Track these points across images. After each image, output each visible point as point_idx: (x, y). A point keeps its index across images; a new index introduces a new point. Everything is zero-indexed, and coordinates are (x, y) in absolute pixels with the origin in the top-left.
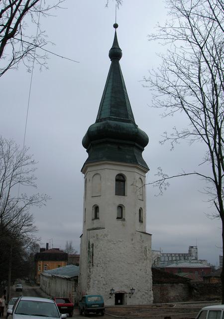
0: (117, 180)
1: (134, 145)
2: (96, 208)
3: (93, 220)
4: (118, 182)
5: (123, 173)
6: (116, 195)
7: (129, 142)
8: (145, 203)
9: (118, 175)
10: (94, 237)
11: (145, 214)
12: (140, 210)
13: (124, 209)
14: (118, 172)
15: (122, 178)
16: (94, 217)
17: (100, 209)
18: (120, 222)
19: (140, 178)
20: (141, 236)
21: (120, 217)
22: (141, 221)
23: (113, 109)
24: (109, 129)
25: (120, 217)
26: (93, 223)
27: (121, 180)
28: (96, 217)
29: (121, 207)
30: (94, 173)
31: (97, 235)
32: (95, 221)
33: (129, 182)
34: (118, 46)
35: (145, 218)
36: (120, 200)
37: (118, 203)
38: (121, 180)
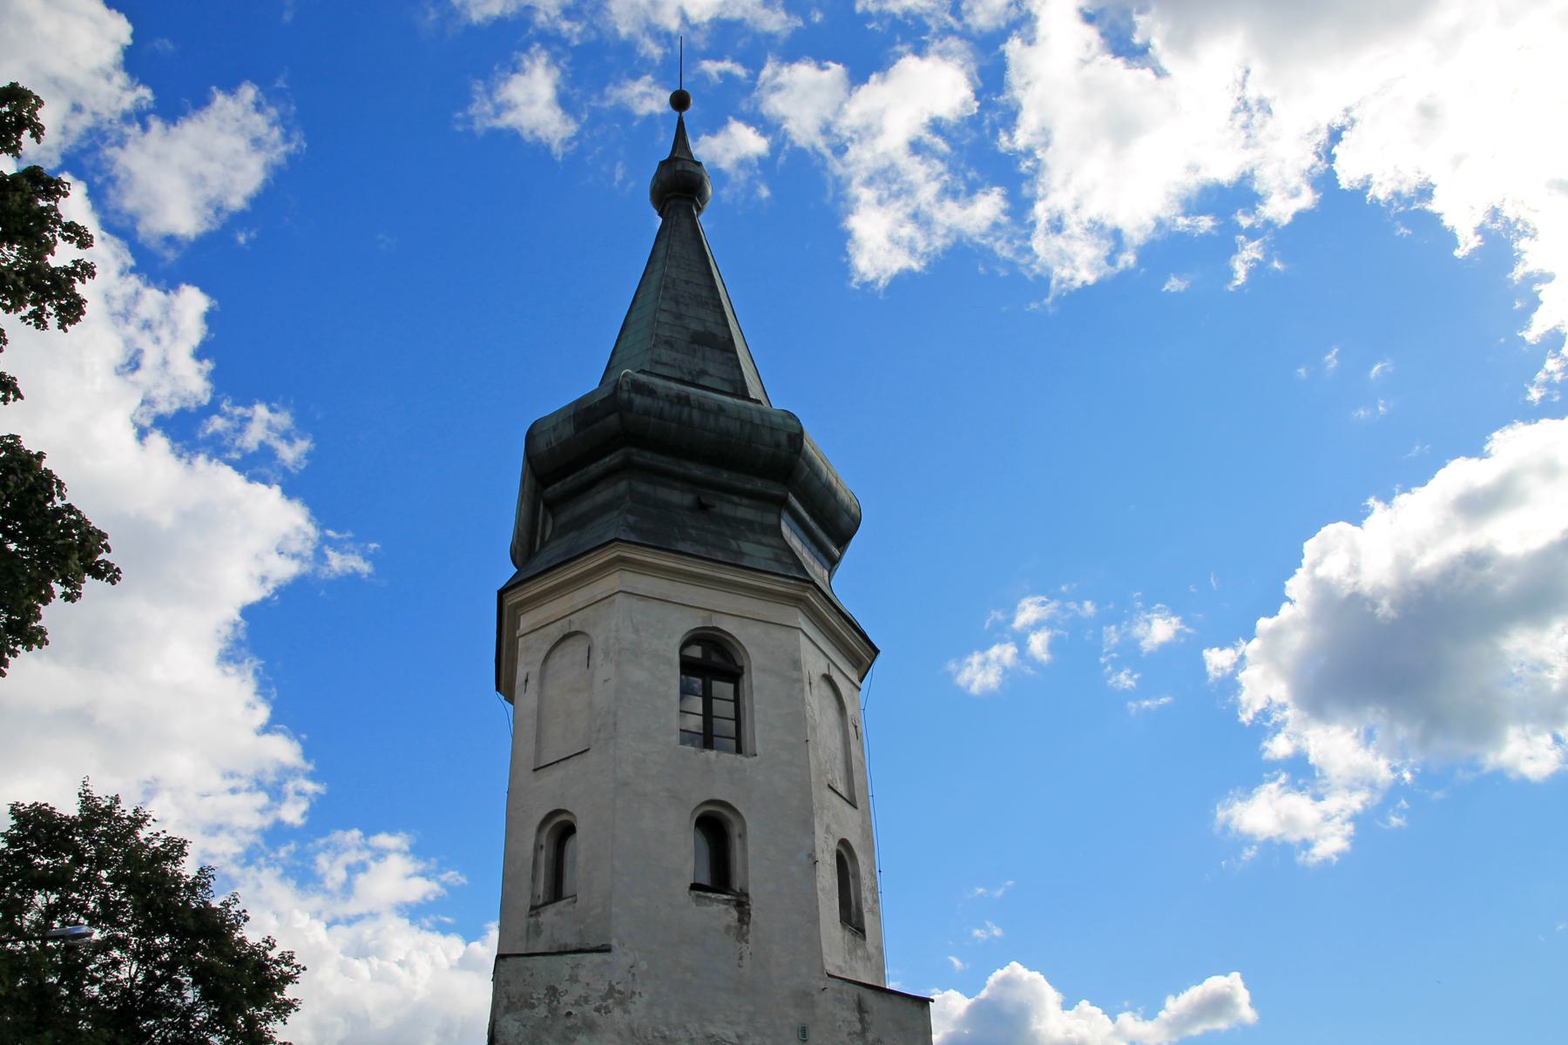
0: (688, 667)
1: (783, 503)
2: (561, 830)
3: (535, 909)
4: (697, 682)
5: (728, 625)
6: (683, 742)
7: (759, 485)
8: (866, 814)
9: (694, 638)
10: (533, 1006)
11: (874, 889)
12: (840, 857)
13: (735, 830)
14: (693, 622)
15: (715, 658)
16: (541, 888)
17: (579, 847)
18: (719, 912)
19: (828, 678)
20: (861, 1008)
21: (719, 876)
22: (852, 917)
23: (666, 354)
24: (640, 401)
25: (719, 876)
26: (537, 930)
27: (711, 662)
28: (556, 891)
29: (715, 828)
30: (555, 632)
31: (553, 992)
32: (549, 915)
33: (760, 681)
34: (690, 155)
35: (876, 913)
36: (716, 777)
37: (698, 794)
38: (711, 662)
